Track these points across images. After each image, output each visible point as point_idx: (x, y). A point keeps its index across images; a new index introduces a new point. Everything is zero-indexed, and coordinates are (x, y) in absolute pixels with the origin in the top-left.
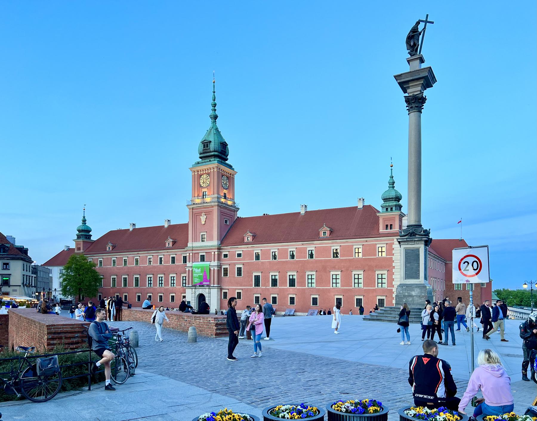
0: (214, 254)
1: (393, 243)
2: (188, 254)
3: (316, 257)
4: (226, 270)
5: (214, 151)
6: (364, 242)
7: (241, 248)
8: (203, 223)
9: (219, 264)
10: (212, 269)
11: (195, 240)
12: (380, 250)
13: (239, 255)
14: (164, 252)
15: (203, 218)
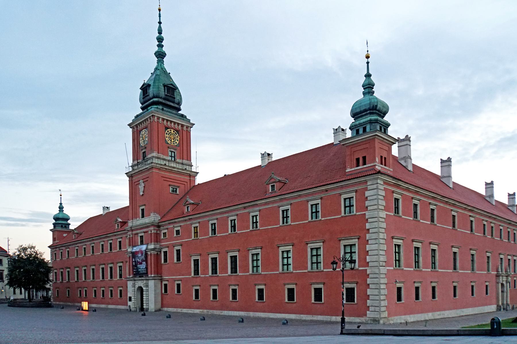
0: (151, 234)
1: (366, 189)
2: (129, 237)
3: (261, 226)
4: (165, 253)
5: (154, 97)
6: (322, 191)
7: (179, 222)
8: (141, 193)
9: (158, 246)
10: (149, 253)
11: (135, 216)
12: (347, 204)
13: (178, 232)
14: (112, 236)
15: (141, 187)
